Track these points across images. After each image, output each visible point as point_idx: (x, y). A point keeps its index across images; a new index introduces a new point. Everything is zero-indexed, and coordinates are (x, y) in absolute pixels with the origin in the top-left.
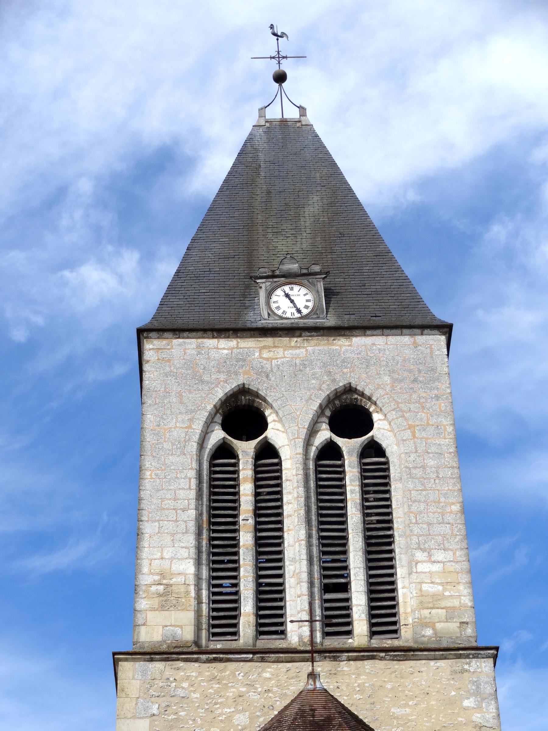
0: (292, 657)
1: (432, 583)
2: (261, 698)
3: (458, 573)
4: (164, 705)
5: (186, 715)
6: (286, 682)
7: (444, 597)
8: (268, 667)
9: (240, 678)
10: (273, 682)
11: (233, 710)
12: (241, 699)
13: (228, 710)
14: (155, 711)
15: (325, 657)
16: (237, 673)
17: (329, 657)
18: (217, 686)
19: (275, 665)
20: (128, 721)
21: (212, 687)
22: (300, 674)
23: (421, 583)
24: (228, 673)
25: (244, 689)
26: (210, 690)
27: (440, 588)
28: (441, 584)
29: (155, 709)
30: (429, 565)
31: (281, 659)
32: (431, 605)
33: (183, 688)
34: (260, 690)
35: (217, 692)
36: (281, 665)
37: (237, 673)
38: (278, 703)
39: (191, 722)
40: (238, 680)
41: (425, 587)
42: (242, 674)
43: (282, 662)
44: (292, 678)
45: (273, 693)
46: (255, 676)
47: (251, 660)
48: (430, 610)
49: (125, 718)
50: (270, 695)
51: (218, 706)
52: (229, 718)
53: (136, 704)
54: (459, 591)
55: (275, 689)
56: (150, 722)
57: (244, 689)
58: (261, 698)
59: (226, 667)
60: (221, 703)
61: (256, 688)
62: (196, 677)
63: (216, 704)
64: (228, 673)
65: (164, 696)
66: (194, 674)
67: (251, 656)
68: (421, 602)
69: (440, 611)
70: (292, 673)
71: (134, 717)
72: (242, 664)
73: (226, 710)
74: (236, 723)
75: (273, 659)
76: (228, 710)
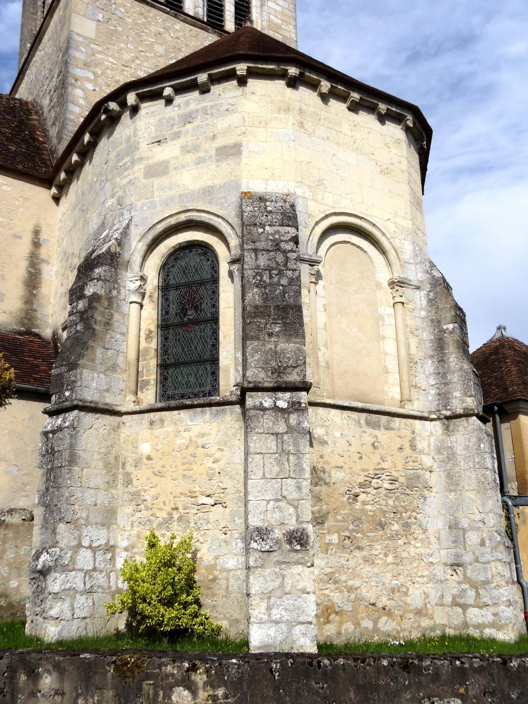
0: (195, 22)
1: (276, 16)
2: (173, 41)
3: (290, 18)
4: (107, 17)
5: (122, 31)
6: (189, 37)
7: (282, 29)
8: (178, 23)
9: (160, 22)
10: (181, 34)
11: (154, 41)
12: (160, 36)
13: (151, 40)
14: (101, 19)
15: (215, 32)
16: (158, 18)
17: (218, 33)
18: (144, 20)
19: (183, 24)
20: (81, 17)
21: (140, 20)
22: (198, 36)
23: (270, 14)
24: (151, 15)
25: (162, 30)
26: (139, 21)
27: (280, 22)
28: (281, 20)
29: (100, 17)
30: (274, 5)
31: (187, 21)
32: (274, 30)
33: (120, 11)
34: (172, 35)
35: (144, 24)
36: (186, 25)
37: (158, 18)
38: (184, 49)
39: (125, 37)
40: (158, 23)
41: (272, 17)
42: (161, 20)
43: (188, 23)
44: (193, 36)
45: (181, 41)
46: (169, 25)
47: (168, 13)
48: (273, 33)
49: (78, 14)
50: (179, 41)
51: (144, 34)
52: (152, 45)
53: (87, 8)
54: (289, 28)
55: (182, 39)
56: (97, 25)
57: (162, 30)
58: (173, 41)
59: (150, 10)
60: (146, 33)
61: (170, 33)
62: (130, 8)
63: (143, 32)
64: (151, 15)
65: (107, 11)
66: (128, 5)
67: (169, 10)
68: (269, 25)
69: (279, 35)
70: (193, 33)
71: (84, 16)
72: (161, 13)
73: (149, 39)
74: (156, 50)
75: (182, 19)
76: (151, 40)
